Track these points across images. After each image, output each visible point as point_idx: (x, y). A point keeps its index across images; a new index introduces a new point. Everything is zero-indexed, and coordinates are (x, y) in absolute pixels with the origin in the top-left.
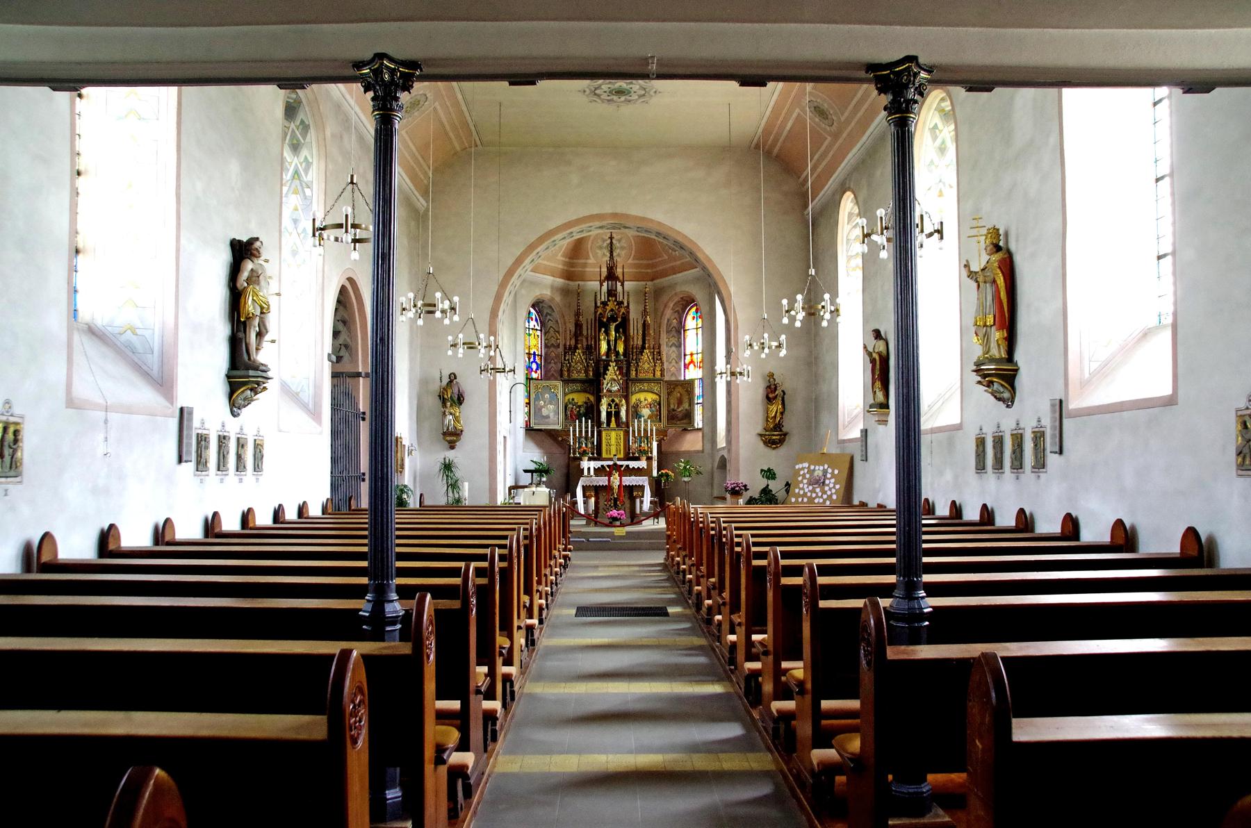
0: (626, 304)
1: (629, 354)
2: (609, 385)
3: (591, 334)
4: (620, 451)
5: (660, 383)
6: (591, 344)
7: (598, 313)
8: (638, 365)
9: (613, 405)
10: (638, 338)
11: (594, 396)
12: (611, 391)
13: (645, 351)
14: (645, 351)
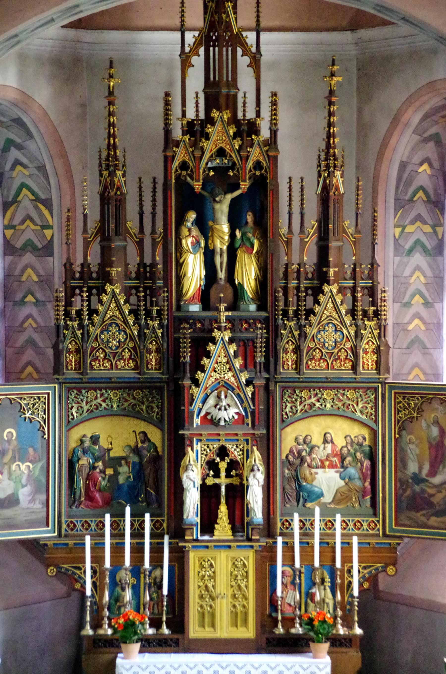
0: (265, 134)
1: (276, 299)
2: (211, 401)
3: (153, 231)
4: (246, 614)
5: (376, 390)
6: (153, 265)
7: (176, 164)
8: (303, 335)
9: (223, 466)
10: (303, 243)
11: (162, 430)
12: (215, 422)
13: (326, 288)
14: (326, 288)
